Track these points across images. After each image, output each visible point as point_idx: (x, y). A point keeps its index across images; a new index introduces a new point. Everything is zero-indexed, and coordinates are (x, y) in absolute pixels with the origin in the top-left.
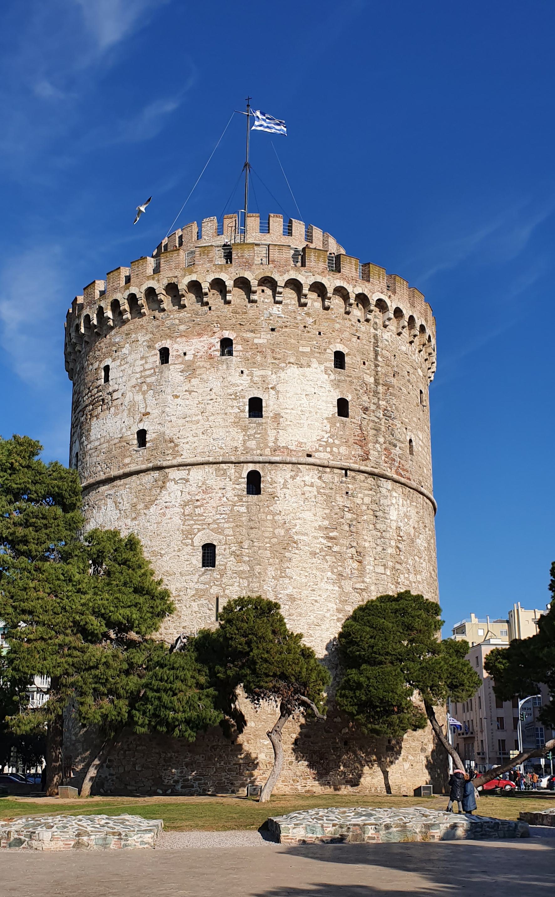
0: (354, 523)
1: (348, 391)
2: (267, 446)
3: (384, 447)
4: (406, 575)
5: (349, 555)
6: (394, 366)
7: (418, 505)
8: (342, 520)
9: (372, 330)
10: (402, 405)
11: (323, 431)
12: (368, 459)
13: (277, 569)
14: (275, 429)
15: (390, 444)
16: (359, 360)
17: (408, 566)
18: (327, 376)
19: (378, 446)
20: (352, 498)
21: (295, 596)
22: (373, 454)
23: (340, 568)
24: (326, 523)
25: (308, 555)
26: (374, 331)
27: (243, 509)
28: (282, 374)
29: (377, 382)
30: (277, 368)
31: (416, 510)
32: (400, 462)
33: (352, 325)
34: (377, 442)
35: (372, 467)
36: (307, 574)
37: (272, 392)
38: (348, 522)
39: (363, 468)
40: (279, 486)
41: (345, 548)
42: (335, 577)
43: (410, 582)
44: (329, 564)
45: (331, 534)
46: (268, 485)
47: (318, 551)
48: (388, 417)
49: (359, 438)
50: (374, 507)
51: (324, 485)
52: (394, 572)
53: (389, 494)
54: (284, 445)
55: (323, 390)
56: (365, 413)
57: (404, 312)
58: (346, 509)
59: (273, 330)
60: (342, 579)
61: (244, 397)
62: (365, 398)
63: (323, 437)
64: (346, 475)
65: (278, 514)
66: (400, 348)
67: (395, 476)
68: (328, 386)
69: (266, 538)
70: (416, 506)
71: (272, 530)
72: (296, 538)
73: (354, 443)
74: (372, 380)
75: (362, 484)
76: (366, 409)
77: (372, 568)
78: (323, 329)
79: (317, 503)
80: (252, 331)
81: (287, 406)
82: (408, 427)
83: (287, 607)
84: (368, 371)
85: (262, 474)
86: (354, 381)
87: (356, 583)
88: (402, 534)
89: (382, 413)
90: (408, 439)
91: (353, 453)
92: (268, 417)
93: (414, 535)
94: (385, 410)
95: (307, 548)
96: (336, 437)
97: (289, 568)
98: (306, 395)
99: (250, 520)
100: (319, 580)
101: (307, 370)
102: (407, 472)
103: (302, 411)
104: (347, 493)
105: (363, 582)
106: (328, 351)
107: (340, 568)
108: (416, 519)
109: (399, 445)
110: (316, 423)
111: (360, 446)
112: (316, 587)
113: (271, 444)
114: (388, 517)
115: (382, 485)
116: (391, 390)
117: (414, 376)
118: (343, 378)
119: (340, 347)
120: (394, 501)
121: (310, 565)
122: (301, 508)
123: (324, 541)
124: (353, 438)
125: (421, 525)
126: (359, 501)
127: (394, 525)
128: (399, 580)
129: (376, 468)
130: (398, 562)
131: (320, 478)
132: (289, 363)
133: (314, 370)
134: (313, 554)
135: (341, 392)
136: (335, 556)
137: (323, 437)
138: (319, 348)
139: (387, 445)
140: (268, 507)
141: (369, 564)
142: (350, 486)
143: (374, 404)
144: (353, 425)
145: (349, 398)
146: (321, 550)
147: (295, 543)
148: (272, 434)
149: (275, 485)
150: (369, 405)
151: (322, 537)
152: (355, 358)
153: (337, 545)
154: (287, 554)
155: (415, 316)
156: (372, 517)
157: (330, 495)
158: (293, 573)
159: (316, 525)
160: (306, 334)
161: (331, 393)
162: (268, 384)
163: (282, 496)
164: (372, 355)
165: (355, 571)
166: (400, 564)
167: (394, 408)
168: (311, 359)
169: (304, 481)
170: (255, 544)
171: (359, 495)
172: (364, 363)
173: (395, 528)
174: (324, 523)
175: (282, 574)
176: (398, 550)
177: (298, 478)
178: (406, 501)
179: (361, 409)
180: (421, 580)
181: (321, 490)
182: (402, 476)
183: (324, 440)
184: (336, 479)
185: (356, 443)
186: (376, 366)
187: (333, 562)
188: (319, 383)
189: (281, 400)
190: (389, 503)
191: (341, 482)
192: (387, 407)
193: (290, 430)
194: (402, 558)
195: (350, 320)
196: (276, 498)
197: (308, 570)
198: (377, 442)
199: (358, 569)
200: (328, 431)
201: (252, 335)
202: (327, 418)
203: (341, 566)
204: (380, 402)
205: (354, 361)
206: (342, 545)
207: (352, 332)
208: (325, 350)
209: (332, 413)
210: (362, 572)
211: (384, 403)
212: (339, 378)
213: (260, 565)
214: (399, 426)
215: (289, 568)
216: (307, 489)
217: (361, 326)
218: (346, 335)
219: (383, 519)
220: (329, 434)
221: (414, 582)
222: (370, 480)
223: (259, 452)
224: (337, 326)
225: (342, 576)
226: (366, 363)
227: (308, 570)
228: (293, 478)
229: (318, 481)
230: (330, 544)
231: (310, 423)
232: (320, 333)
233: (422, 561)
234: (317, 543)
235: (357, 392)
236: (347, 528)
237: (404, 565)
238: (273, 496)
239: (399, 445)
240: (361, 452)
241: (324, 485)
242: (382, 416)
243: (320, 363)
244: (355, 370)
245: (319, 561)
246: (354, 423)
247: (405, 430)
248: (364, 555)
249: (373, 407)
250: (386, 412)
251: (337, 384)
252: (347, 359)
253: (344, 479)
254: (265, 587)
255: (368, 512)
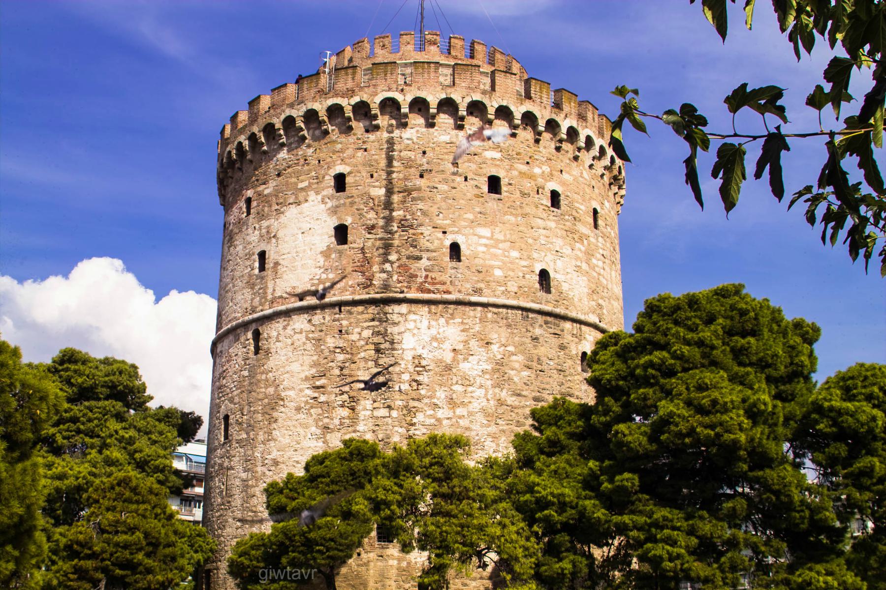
0: (347, 364)
1: (347, 215)
2: (266, 299)
3: (396, 265)
4: (432, 412)
5: (338, 403)
6: (421, 165)
7: (465, 321)
8: (331, 364)
9: (386, 135)
10: (436, 207)
11: (316, 267)
12: (371, 284)
13: (265, 433)
14: (273, 279)
15: (407, 258)
16: (364, 174)
17: (435, 401)
18: (324, 205)
19: (388, 266)
20: (346, 336)
21: (278, 460)
22: (379, 279)
23: (326, 420)
24: (313, 371)
25: (293, 411)
26: (388, 135)
27: (246, 373)
28: (283, 219)
29: (390, 192)
30: (279, 212)
31: (462, 327)
32: (427, 277)
33: (358, 139)
34: (387, 261)
35: (378, 293)
36: (291, 433)
37: (274, 240)
38: (339, 364)
39: (357, 297)
40: (272, 341)
41: (334, 395)
42: (320, 431)
43: (439, 420)
44: (314, 416)
45: (318, 383)
46: (265, 342)
47: (303, 405)
48: (408, 227)
49: (359, 264)
50: (376, 339)
51: (313, 329)
52: (405, 412)
53: (400, 319)
54: (280, 294)
55: (318, 222)
56: (370, 233)
57: (429, 99)
58: (338, 350)
59: (279, 175)
60: (328, 432)
61: (253, 254)
62: (372, 215)
63: (316, 274)
64: (340, 311)
65: (271, 372)
66: (435, 140)
67: (411, 295)
68: (325, 216)
69: (260, 400)
70: (462, 323)
71: (263, 390)
72: (283, 394)
73: (353, 271)
74: (383, 191)
75: (359, 317)
76: (371, 228)
77: (369, 413)
78: (322, 155)
79: (305, 350)
80: (264, 184)
81: (285, 252)
82: (448, 230)
83: (271, 473)
84: (377, 184)
85: (261, 331)
86: (356, 200)
87: (345, 434)
88: (424, 363)
89: (395, 225)
90: (448, 243)
91: (350, 283)
92: (268, 269)
93: (454, 359)
94: (402, 220)
95: (292, 403)
96: (330, 270)
97: (275, 429)
98: (303, 233)
99: (251, 383)
100: (302, 438)
101: (305, 206)
102: (444, 284)
103: (297, 252)
104: (341, 331)
105: (354, 431)
106: (327, 177)
107: (326, 420)
108: (463, 338)
109: (425, 255)
110: (309, 261)
111: (361, 272)
112: (298, 446)
113: (270, 297)
114: (396, 346)
115: (391, 311)
116: (415, 194)
117: (470, 164)
118: (342, 202)
119: (340, 169)
120: (411, 325)
121: (294, 423)
122: (290, 360)
123: (309, 392)
124: (352, 265)
125: (473, 343)
126: (355, 337)
127: (408, 356)
128: (414, 420)
129: (383, 292)
130: (413, 399)
131: (310, 321)
132: (289, 204)
133: (312, 203)
134: (298, 409)
135: (339, 218)
136: (321, 407)
137: (316, 274)
138: (317, 178)
139: (404, 260)
140: (263, 366)
141: (365, 409)
142: (345, 323)
143: (384, 218)
144: (352, 251)
145: (348, 221)
146: (307, 402)
147: (283, 400)
148: (270, 285)
149: (269, 340)
150: (375, 222)
151: (308, 388)
152: (359, 175)
153: (324, 394)
154: (275, 414)
155: (453, 96)
156: (373, 352)
157: (319, 338)
158: (278, 434)
159: (303, 376)
160: (306, 168)
161: (327, 223)
162: (272, 232)
163: (275, 350)
164: (383, 163)
165: (345, 421)
166: (419, 400)
167: (419, 214)
168: (309, 193)
169: (294, 329)
170: (252, 409)
171: (358, 330)
172: (372, 176)
173: (411, 358)
174: (311, 372)
175: (270, 438)
176: (414, 384)
177: (289, 328)
178: (437, 320)
179: (365, 230)
180: (465, 413)
181: (311, 335)
182: (429, 291)
183: (318, 277)
184: (328, 318)
185: (356, 271)
186: (389, 173)
187: (319, 415)
188: (315, 216)
189: (280, 247)
190: (403, 330)
191: (333, 321)
192: (405, 216)
193: (285, 276)
194: (423, 392)
195: (354, 135)
196: (270, 355)
197: (292, 428)
198: (387, 261)
199: (349, 418)
200: (322, 266)
201: (264, 186)
202: (321, 253)
203: (327, 417)
204: (395, 214)
205: (358, 178)
206: (330, 393)
207: (357, 146)
208: (324, 177)
209: (326, 244)
210: (354, 419)
211: (401, 213)
212: (337, 204)
213: (254, 431)
214: (426, 233)
215: (275, 429)
216: (297, 336)
217: (370, 136)
218: (349, 152)
219: (390, 351)
220: (322, 270)
221: (448, 418)
222: (372, 310)
223: (261, 308)
224: (339, 146)
225: (328, 428)
226: (375, 175)
227: (292, 428)
228: (285, 328)
229: (308, 325)
230: (316, 395)
231: (303, 262)
232: (319, 161)
233: (470, 389)
234: (303, 396)
235: (359, 212)
236: (337, 372)
237: (426, 401)
238: (268, 352)
239: (425, 255)
240: (360, 279)
241: (313, 329)
242: (395, 229)
243: (317, 193)
244: (359, 188)
245: (303, 416)
246: (353, 248)
247: (440, 235)
248: (358, 400)
249: (381, 222)
250: (403, 222)
251: (334, 211)
252: (349, 180)
253: (337, 316)
254: (256, 454)
255: (367, 347)
